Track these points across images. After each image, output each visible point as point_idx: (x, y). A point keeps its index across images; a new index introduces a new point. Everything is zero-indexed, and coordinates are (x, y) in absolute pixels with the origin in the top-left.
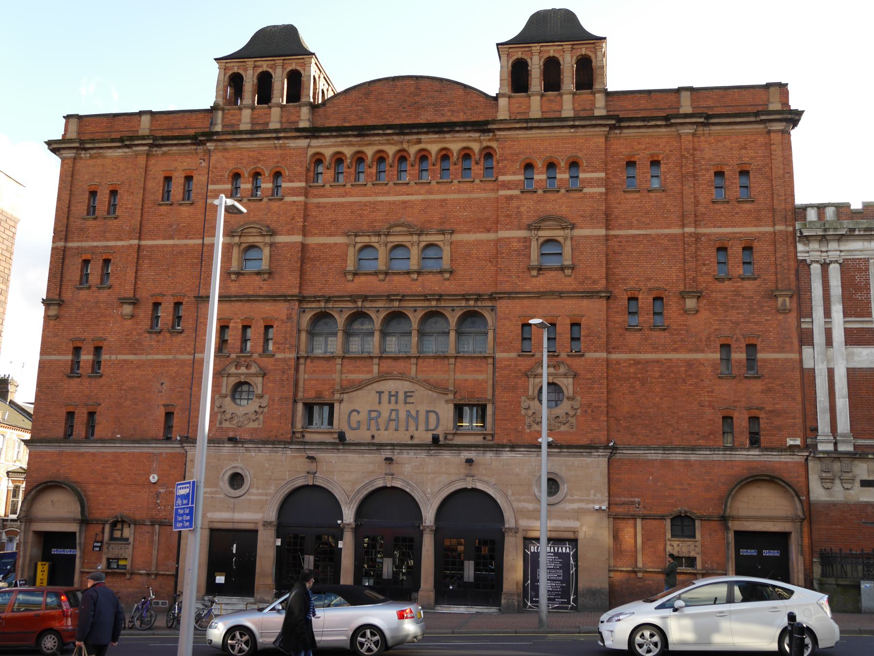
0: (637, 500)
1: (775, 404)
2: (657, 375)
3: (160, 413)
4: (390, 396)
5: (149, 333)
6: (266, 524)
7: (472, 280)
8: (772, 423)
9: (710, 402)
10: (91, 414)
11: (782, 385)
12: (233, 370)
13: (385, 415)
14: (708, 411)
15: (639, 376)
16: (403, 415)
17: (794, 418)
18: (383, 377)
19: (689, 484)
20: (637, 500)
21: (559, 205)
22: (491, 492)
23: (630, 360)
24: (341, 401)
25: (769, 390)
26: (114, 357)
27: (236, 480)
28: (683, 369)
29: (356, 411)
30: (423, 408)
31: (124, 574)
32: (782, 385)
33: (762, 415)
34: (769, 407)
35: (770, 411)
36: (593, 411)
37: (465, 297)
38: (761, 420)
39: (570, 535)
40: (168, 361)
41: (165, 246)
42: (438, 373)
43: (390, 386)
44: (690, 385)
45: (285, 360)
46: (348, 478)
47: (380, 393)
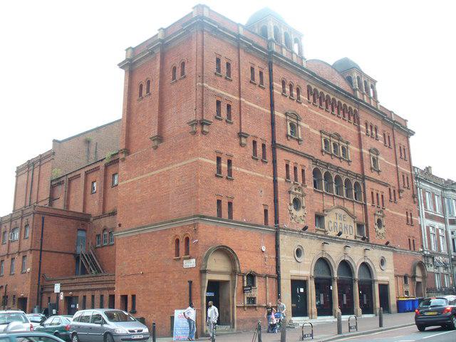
3: (262, 209)
5: (253, 158)
7: (354, 168)
10: (230, 204)
12: (293, 190)
13: (339, 224)
18: (339, 207)
21: (374, 144)
22: (370, 264)
26: (238, 169)
27: (299, 253)
29: (330, 220)
30: (349, 224)
31: (256, 307)
37: (357, 176)
39: (387, 283)
40: (262, 178)
41: (255, 108)
42: (348, 206)
43: (340, 211)
45: (310, 190)
46: (335, 254)
47: (336, 214)
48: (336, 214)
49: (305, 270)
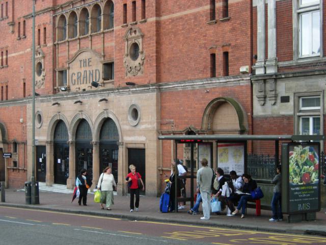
0: (172, 120)
1: (236, 40)
2: (181, 28)
4: (84, 62)
6: (47, 142)
8: (235, 56)
9: (205, 44)
11: (240, 24)
14: (204, 50)
15: (173, 30)
16: (88, 73)
17: (246, 50)
19: (195, 108)
20: (172, 120)
23: (170, 19)
24: (69, 68)
25: (233, 29)
28: (193, 21)
32: (240, 24)
33: (230, 51)
34: (233, 43)
35: (235, 46)
36: (150, 60)
38: (229, 54)
44: (196, 32)
47: (81, 61)
48: (81, 61)
49: (43, 137)
